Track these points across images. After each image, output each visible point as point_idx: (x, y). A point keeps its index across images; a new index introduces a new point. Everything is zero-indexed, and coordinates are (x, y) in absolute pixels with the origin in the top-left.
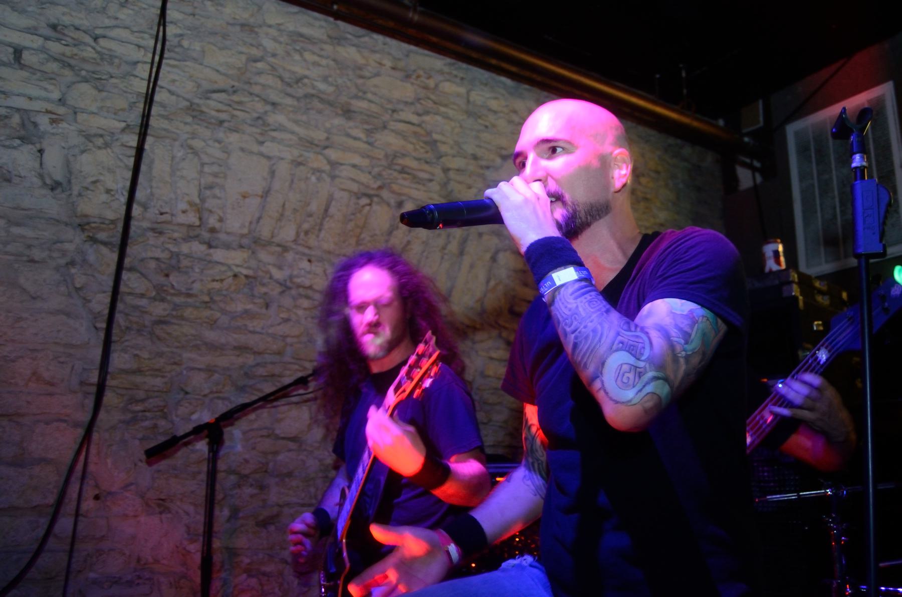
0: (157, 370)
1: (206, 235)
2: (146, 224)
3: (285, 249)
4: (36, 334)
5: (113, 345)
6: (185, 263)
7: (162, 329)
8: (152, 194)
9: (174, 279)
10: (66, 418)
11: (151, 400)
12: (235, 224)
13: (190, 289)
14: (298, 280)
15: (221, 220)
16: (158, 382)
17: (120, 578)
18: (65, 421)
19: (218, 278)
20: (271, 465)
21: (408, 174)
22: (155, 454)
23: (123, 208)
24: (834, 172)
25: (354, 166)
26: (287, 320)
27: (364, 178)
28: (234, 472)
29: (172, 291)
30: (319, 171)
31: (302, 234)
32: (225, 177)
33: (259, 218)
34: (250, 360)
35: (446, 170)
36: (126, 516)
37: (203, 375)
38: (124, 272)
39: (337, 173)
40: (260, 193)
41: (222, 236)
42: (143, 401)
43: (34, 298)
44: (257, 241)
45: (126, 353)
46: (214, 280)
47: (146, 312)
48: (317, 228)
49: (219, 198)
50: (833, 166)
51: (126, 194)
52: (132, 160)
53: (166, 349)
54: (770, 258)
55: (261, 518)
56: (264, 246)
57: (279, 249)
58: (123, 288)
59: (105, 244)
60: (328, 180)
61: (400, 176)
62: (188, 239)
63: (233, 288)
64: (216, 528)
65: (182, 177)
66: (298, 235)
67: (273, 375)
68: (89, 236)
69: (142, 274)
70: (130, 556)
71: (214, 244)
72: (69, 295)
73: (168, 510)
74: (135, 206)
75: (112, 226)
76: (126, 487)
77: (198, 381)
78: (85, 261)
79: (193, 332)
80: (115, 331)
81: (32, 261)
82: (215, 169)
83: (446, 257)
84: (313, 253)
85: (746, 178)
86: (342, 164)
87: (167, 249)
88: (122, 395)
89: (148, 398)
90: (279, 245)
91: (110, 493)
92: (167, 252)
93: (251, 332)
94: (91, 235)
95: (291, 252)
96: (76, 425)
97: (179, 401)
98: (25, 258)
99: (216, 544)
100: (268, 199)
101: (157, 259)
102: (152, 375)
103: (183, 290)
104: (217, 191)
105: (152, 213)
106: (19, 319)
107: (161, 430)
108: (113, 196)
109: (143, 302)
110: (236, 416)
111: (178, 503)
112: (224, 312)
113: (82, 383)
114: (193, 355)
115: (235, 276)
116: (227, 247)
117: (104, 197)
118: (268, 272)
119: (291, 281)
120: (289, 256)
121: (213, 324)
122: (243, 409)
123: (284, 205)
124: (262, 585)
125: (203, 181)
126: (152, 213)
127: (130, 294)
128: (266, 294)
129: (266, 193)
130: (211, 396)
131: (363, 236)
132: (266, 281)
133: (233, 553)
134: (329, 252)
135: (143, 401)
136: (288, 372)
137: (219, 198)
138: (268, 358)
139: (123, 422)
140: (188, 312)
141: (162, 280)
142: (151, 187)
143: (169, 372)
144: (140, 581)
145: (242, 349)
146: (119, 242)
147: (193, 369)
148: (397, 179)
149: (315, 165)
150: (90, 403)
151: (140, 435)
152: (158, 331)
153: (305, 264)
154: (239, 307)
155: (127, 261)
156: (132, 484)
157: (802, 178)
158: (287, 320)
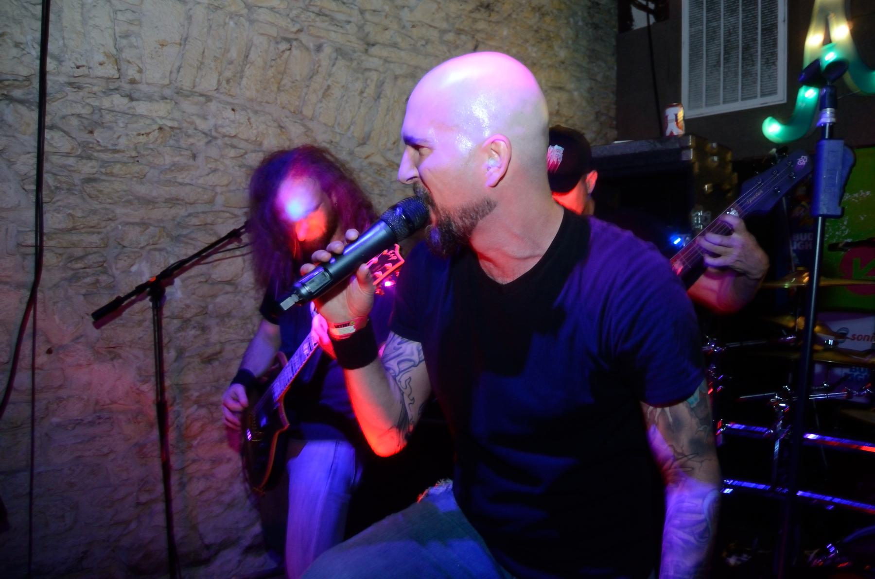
0: (92, 227)
1: (127, 87)
2: (62, 79)
3: (209, 99)
5: (44, 205)
6: (108, 117)
7: (93, 187)
8: (65, 45)
9: (100, 135)
10: (8, 280)
11: (90, 257)
12: (155, 74)
13: (116, 145)
14: (224, 130)
15: (140, 71)
16: (95, 239)
17: (82, 420)
19: (143, 132)
20: (211, 307)
21: (326, 16)
22: (102, 316)
23: (38, 62)
24: (722, 20)
25: (272, 9)
26: (215, 171)
27: (283, 22)
28: (177, 317)
29: (99, 148)
30: (237, 15)
31: (224, 82)
32: (140, 24)
33: (180, 67)
34: (182, 212)
35: (362, 12)
36: (80, 366)
37: (138, 229)
38: (46, 131)
39: (255, 16)
40: (178, 41)
41: (143, 87)
42: (81, 258)
44: (179, 92)
45: (59, 213)
46: (139, 135)
47: (74, 171)
48: (238, 75)
49: (136, 47)
50: (722, 14)
51: (38, 48)
52: (40, 8)
53: (98, 207)
54: (672, 121)
55: (206, 355)
56: (188, 96)
57: (202, 99)
58: (47, 148)
59: (22, 102)
60: (246, 24)
61: (318, 19)
62: (108, 92)
63: (159, 141)
64: (166, 367)
65: (96, 26)
66: (219, 83)
67: (206, 224)
68: (3, 94)
69: (67, 133)
70: (88, 400)
71: (135, 96)
73: (119, 356)
74: (49, 60)
75: (27, 83)
76: (76, 339)
77: (133, 235)
79: (125, 187)
80: (45, 192)
82: (129, 15)
83: (365, 100)
84: (236, 101)
85: (640, 19)
86: (260, 7)
87: (88, 104)
89: (87, 255)
90: (201, 95)
91: (61, 347)
92: (88, 107)
93: (181, 184)
94: (5, 92)
95: (214, 102)
96: (19, 286)
97: (118, 255)
99: (168, 383)
100: (187, 47)
101: (79, 116)
102: (86, 233)
103: (111, 147)
104: (133, 40)
105: (68, 66)
107: (103, 285)
108: (23, 49)
109: (71, 161)
110: (175, 272)
111: (128, 349)
112: (152, 166)
113: (19, 245)
115: (160, 129)
116: (150, 98)
117: (14, 52)
118: (192, 123)
119: (216, 131)
120: (213, 106)
121: (141, 178)
122: (181, 267)
123: (204, 52)
124: (211, 413)
125: (117, 29)
126: (68, 66)
127: (55, 153)
128: (192, 144)
129: (184, 40)
130: (148, 248)
131: (283, 82)
132: (190, 132)
133: (183, 389)
134: (251, 100)
135: (81, 258)
136: (220, 220)
137: (136, 47)
138: (200, 208)
139: (65, 279)
140: (117, 169)
141: (85, 136)
142: (63, 38)
143: (105, 227)
144: (101, 421)
145: (173, 201)
146: (37, 100)
147: (127, 224)
148: (314, 21)
149: (233, 9)
150: (30, 263)
151: (83, 291)
152: (88, 188)
153: (229, 114)
154: (168, 160)
155: (48, 120)
156: (82, 336)
157: (692, 24)
158: (215, 171)
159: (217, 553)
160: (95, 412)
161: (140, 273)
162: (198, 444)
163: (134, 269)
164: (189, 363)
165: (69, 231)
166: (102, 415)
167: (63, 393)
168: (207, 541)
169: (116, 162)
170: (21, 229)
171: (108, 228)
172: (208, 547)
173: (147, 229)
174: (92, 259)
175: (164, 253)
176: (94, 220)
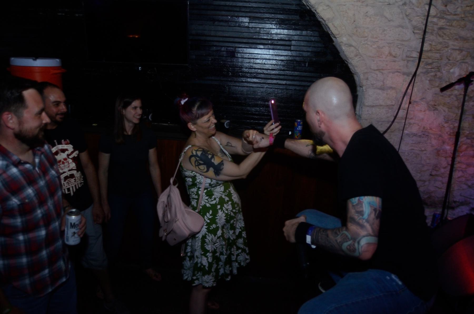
4: (390, 36)
10: (400, 71)
11: (434, 64)
16: (437, 55)
18: (399, 72)
19: (469, 5)
36: (421, 111)
37: (458, 52)
42: (431, 64)
43: (389, 21)
46: (467, 6)
53: (441, 41)
72: (403, 18)
73: (436, 109)
81: (389, 4)
88: (423, 62)
89: (433, 62)
91: (415, 101)
96: (404, 74)
98: (386, 3)
102: (436, 53)
103: (453, 13)
107: (438, 76)
113: (407, 56)
114: (455, 43)
124: (472, 142)
151: (429, 79)
152: (440, 33)
156: (424, 98)
159: (458, 206)
160: (422, 132)
161: (454, 73)
162: (462, 155)
163: (452, 71)
164: (467, 118)
165: (427, 51)
166: (425, 134)
167: (412, 121)
168: (455, 200)
169: (454, 20)
170: (409, 49)
171: (444, 51)
172: (455, 202)
173: (462, 52)
174: (435, 65)
175: (467, 64)
176: (439, 47)
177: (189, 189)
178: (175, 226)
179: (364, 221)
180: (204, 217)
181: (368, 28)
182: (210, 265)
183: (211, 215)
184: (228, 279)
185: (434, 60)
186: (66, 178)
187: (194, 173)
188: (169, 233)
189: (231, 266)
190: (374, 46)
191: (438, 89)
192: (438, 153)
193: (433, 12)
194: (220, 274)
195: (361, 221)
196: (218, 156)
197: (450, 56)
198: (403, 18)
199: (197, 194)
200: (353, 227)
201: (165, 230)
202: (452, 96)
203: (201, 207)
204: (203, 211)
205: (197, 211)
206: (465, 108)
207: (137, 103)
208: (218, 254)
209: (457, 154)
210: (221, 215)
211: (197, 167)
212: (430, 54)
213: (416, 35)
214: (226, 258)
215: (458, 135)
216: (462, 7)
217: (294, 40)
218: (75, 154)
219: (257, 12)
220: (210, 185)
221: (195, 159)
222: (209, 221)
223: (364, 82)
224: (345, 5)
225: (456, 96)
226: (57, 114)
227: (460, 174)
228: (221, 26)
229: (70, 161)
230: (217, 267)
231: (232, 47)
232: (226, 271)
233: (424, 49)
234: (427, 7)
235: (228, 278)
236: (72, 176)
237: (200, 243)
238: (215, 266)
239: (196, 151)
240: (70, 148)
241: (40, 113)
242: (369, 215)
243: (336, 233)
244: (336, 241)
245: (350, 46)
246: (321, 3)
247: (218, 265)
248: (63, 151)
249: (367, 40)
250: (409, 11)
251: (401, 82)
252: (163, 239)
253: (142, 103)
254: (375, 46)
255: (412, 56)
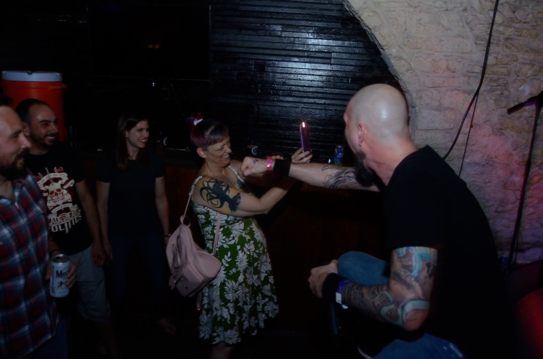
11: (500, 80)
16: (504, 70)
17: (479, 163)
18: (458, 90)
37: (528, 67)
42: (496, 80)
43: (447, 30)
46: (539, 13)
73: (503, 134)
78: (472, 7)
88: (487, 78)
89: (499, 79)
96: (465, 92)
103: (522, 20)
106: (441, 41)
111: (509, 131)
139: (485, 91)
147: (523, 63)
151: (494, 98)
156: (488, 121)
159: (528, 249)
160: (486, 160)
161: (524, 91)
163: (521, 88)
165: (493, 65)
166: (489, 163)
167: (474, 148)
169: (524, 29)
171: (512, 65)
174: (501, 81)
177: (203, 228)
178: (185, 271)
179: (413, 279)
180: (221, 261)
181: (422, 38)
182: (233, 317)
183: (229, 258)
184: (254, 334)
185: (500, 76)
186: (59, 213)
187: (206, 208)
188: (180, 279)
189: (257, 318)
190: (429, 60)
191: (505, 111)
192: (505, 185)
193: (498, 19)
194: (245, 328)
195: (408, 280)
196: (235, 188)
197: (519, 72)
198: (463, 27)
199: (213, 234)
200: (396, 286)
201: (175, 277)
202: (522, 119)
203: (217, 249)
204: (220, 254)
205: (212, 254)
206: (537, 132)
207: (142, 124)
208: (240, 304)
209: (527, 187)
210: (242, 259)
211: (209, 202)
212: (495, 69)
213: (479, 46)
214: (250, 308)
215: (528, 165)
216: (533, 13)
217: (334, 52)
218: (71, 183)
219: (291, 19)
220: (227, 222)
221: (207, 192)
222: (227, 265)
223: (417, 102)
224: (394, 11)
225: (526, 118)
226: (46, 135)
227: (532, 210)
228: (249, 35)
229: (65, 192)
230: (240, 319)
231: (262, 60)
232: (251, 324)
233: (488, 63)
234: (492, 14)
235: (253, 332)
236: (67, 210)
237: (218, 292)
238: (238, 318)
239: (208, 182)
240: (64, 176)
241: (16, 135)
242: (420, 272)
243: (373, 292)
244: (374, 303)
245: (401, 58)
246: (365, 8)
247: (241, 317)
248: (56, 180)
249: (420, 52)
250: (470, 18)
251: (462, 101)
252: (172, 288)
253: (150, 124)
254: (430, 59)
255: (474, 70)
